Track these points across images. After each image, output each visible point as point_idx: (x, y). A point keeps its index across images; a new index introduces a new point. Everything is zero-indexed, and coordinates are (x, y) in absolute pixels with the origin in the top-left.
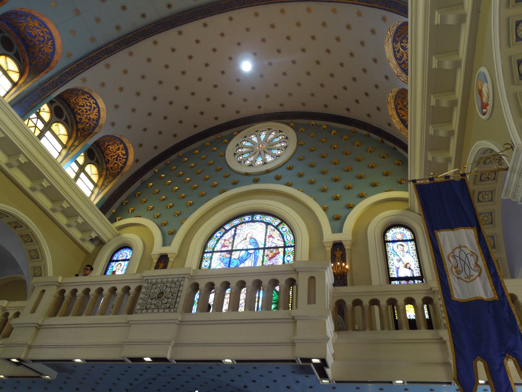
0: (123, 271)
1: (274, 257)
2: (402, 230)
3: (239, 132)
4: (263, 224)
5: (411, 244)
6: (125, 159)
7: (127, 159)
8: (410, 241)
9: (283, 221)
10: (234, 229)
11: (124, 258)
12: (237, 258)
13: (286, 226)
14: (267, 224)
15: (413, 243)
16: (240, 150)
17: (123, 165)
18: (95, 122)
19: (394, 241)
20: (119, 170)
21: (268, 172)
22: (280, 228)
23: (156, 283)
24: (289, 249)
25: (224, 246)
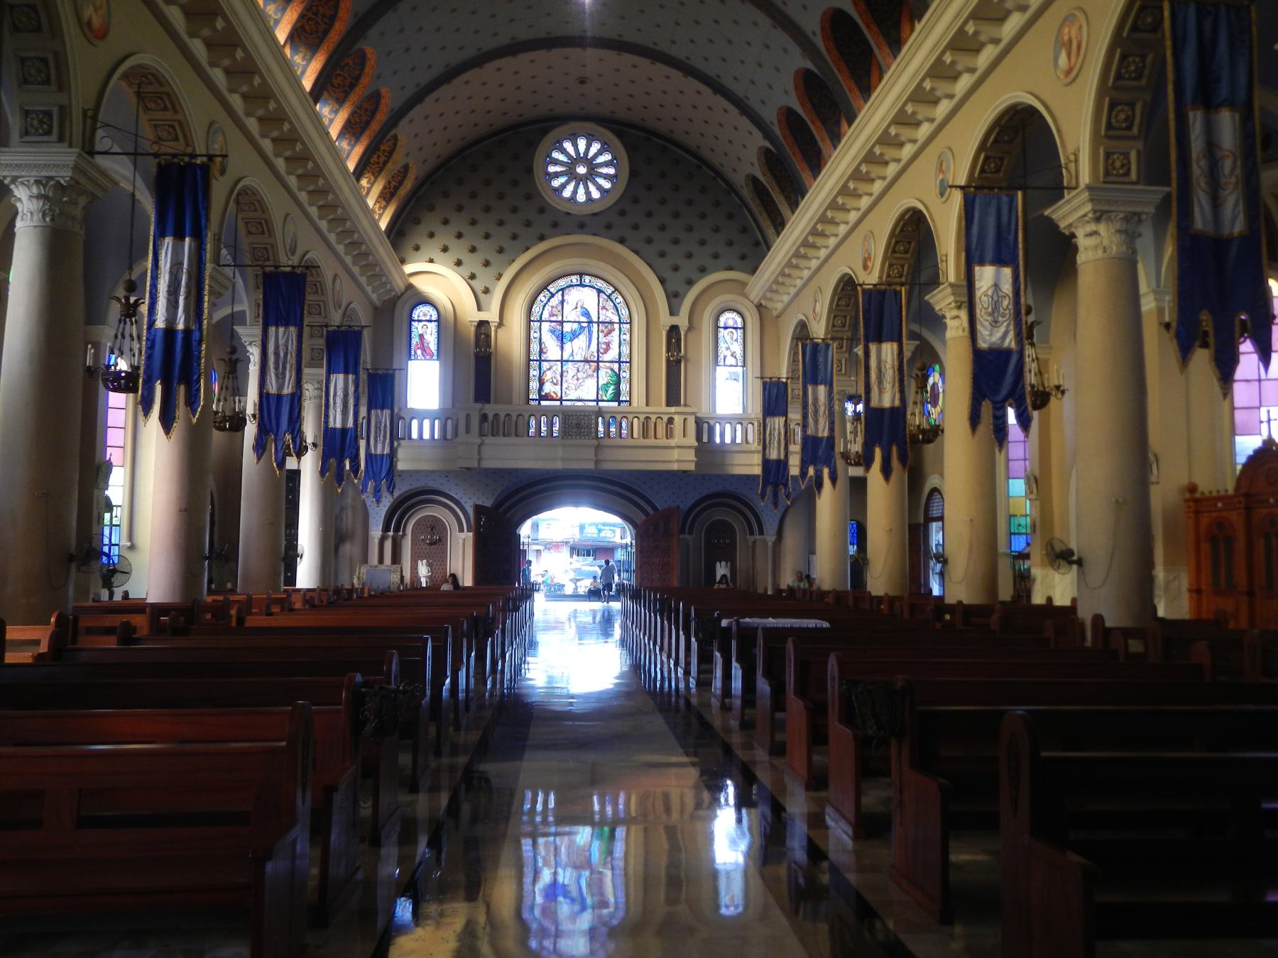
2: (734, 315)
3: (545, 132)
4: (594, 290)
5: (740, 332)
7: (404, 177)
11: (428, 318)
12: (569, 331)
13: (620, 297)
14: (599, 291)
15: (742, 331)
16: (552, 167)
19: (726, 328)
20: (392, 190)
21: (595, 215)
22: (613, 297)
24: (625, 325)
25: (552, 315)
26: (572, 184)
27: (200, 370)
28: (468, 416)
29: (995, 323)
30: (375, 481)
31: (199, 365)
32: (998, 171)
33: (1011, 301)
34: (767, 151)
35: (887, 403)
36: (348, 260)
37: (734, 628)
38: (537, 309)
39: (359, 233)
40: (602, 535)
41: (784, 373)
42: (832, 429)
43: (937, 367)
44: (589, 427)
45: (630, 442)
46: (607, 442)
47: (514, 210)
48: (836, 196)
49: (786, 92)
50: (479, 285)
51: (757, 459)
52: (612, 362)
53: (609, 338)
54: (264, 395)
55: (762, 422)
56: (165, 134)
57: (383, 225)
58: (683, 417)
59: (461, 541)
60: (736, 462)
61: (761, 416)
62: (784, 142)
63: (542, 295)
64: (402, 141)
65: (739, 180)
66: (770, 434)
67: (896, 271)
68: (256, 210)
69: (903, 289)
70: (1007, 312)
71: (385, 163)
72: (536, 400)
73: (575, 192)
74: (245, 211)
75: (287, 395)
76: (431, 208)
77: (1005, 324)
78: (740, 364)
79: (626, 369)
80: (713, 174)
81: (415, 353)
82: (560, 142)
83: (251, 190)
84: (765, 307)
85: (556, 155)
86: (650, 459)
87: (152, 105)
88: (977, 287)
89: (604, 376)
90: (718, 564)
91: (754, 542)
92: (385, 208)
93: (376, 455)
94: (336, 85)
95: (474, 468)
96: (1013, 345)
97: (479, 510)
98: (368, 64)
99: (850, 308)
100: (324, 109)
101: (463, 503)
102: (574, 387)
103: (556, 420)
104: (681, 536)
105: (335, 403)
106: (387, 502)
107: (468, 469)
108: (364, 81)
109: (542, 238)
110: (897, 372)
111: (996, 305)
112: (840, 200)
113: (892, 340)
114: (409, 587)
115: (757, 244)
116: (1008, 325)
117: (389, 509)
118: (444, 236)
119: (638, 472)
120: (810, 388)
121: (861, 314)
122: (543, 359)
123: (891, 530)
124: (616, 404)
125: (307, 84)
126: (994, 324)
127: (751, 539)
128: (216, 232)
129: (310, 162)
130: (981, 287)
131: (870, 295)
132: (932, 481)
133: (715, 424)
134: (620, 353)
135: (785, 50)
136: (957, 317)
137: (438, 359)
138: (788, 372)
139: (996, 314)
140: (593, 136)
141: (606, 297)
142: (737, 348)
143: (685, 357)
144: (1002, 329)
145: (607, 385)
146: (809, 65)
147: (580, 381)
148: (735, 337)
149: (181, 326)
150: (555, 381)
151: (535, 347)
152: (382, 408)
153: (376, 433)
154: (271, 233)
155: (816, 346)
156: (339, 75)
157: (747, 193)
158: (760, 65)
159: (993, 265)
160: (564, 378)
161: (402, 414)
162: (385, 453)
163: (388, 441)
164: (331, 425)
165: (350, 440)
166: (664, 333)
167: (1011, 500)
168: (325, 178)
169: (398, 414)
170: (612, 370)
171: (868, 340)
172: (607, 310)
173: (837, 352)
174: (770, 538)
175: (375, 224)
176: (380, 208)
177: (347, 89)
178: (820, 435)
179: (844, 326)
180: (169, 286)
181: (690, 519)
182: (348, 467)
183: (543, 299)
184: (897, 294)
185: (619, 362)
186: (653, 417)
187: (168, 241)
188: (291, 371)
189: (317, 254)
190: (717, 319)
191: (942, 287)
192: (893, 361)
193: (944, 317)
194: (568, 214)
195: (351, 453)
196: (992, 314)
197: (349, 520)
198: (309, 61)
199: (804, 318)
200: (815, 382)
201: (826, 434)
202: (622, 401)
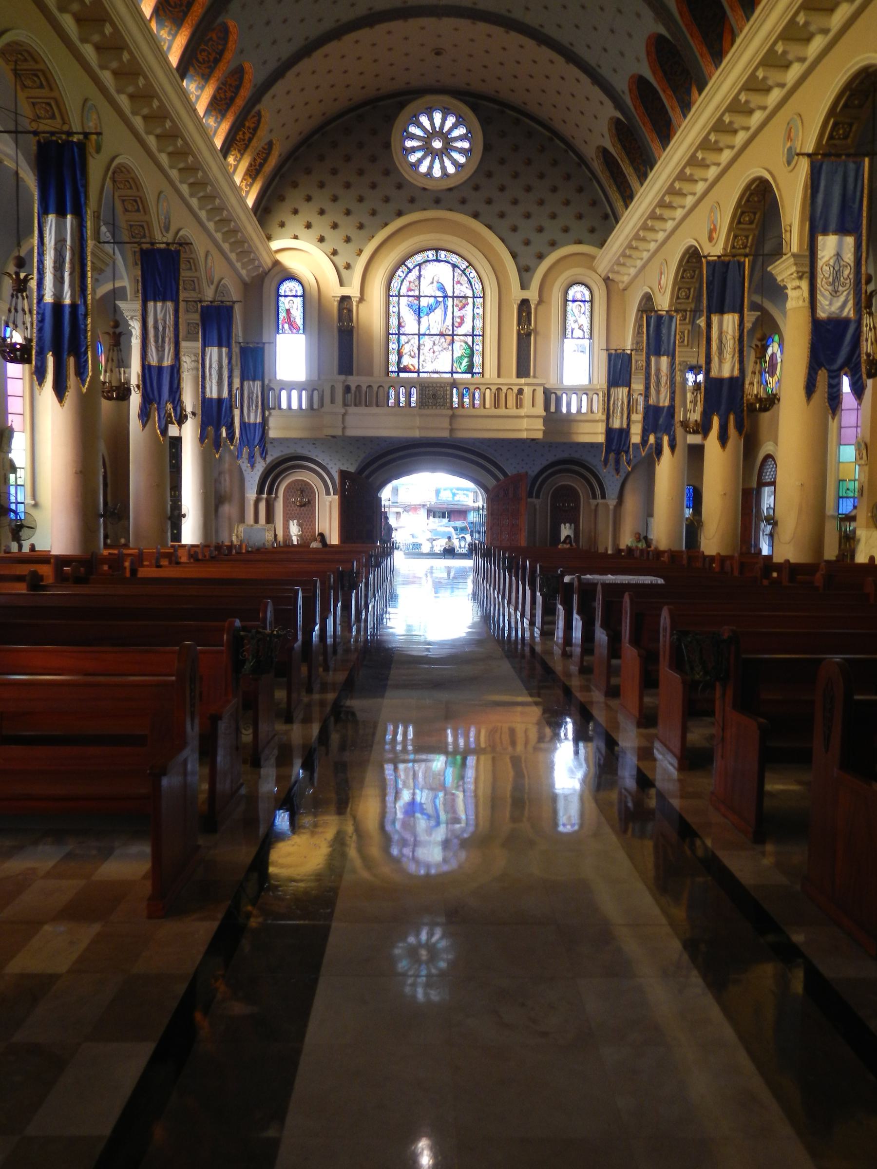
0: (299, 310)
1: (464, 308)
3: (402, 106)
4: (449, 265)
5: (588, 305)
6: (266, 153)
7: (268, 154)
8: (588, 302)
9: (470, 264)
10: (418, 267)
11: (294, 293)
12: (426, 305)
13: (474, 272)
14: (454, 266)
15: (589, 304)
16: (409, 142)
17: (262, 161)
18: (251, 131)
19: (574, 301)
21: (450, 189)
22: (467, 272)
23: (428, 387)
25: (409, 290)
26: (429, 159)
27: (87, 342)
28: (333, 388)
29: (835, 293)
30: (249, 448)
31: (86, 338)
32: (846, 137)
33: (852, 271)
34: (618, 119)
35: (726, 374)
36: (219, 236)
37: (576, 583)
38: (396, 285)
39: (228, 210)
40: (456, 498)
41: (628, 345)
42: (672, 399)
43: (776, 338)
44: (444, 397)
45: (483, 412)
46: (461, 412)
47: (374, 186)
48: (684, 167)
49: (638, 60)
50: (340, 261)
51: (601, 428)
52: (466, 335)
53: (463, 312)
54: (147, 367)
55: (606, 392)
56: (43, 112)
57: (250, 202)
58: (532, 388)
59: (328, 504)
60: (581, 431)
61: (605, 386)
62: (635, 113)
63: (400, 270)
64: (266, 116)
65: (590, 153)
66: (614, 403)
67: (740, 242)
68: (131, 188)
69: (747, 260)
70: (848, 281)
71: (250, 140)
72: (395, 372)
73: (431, 167)
74: (121, 189)
75: (167, 366)
76: (295, 185)
77: (845, 293)
78: (587, 336)
79: (479, 343)
80: (563, 146)
81: (283, 327)
82: (416, 116)
83: (125, 168)
84: (613, 280)
85: (413, 129)
86: (502, 427)
87: (28, 83)
88: (819, 257)
89: (459, 349)
90: (563, 526)
91: (597, 505)
92: (251, 185)
93: (249, 424)
94: (201, 60)
95: (340, 437)
96: (852, 315)
97: (344, 474)
98: (231, 38)
99: (694, 280)
100: (190, 86)
101: (330, 470)
102: (430, 360)
103: (414, 391)
104: (529, 500)
105: (210, 374)
106: (260, 466)
107: (334, 437)
108: (228, 55)
109: (400, 214)
110: (737, 343)
111: (837, 275)
112: (688, 171)
113: (733, 311)
114: (282, 544)
115: (606, 217)
116: (848, 294)
117: (262, 474)
118: (308, 213)
119: (490, 440)
120: (653, 359)
121: (705, 285)
122: (401, 332)
123: (725, 494)
124: (470, 375)
125: (174, 59)
126: (834, 294)
127: (593, 502)
128: (96, 210)
129: (180, 140)
130: (823, 257)
131: (714, 267)
132: (767, 448)
133: (562, 394)
134: (473, 327)
135: (638, 15)
136: (799, 287)
137: (304, 333)
138: (632, 344)
139: (836, 284)
140: (448, 109)
141: (460, 272)
142: (585, 321)
143: (535, 330)
144: (842, 299)
145: (461, 358)
146: (662, 31)
147: (436, 354)
148: (582, 311)
149: (67, 301)
150: (413, 354)
151: (394, 321)
152: (254, 380)
153: (249, 403)
154: (146, 211)
155: (660, 318)
156: (204, 50)
157: (597, 166)
158: (612, 31)
159: (836, 235)
160: (421, 352)
161: (272, 385)
162: (258, 421)
163: (260, 410)
164: (208, 395)
165: (226, 409)
166: (515, 307)
167: (841, 466)
168: (194, 156)
169: (268, 385)
170: (466, 343)
171: (710, 312)
172: (461, 284)
173: (679, 324)
174: (612, 503)
175: (242, 201)
176: (246, 185)
177: (213, 65)
178: (661, 405)
179: (688, 298)
180: (55, 262)
181: (538, 483)
182: (224, 435)
183: (401, 274)
184: (741, 265)
185: (473, 335)
186: (504, 389)
187: (51, 218)
188: (169, 344)
189: (190, 232)
190: (566, 293)
191: (784, 257)
192: (734, 332)
193: (785, 287)
194: (424, 189)
195: (227, 421)
196: (833, 284)
197: (226, 483)
198: (175, 36)
199: (650, 291)
200: (658, 354)
201: (667, 404)
202: (476, 373)
